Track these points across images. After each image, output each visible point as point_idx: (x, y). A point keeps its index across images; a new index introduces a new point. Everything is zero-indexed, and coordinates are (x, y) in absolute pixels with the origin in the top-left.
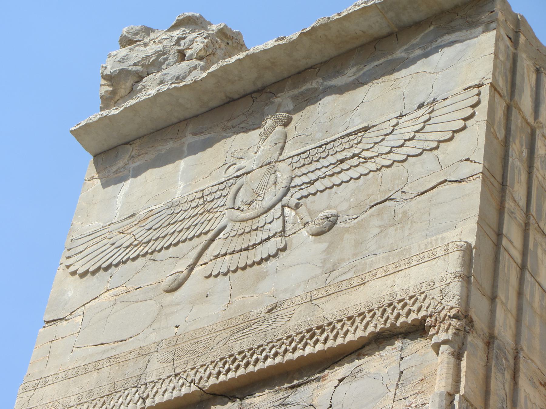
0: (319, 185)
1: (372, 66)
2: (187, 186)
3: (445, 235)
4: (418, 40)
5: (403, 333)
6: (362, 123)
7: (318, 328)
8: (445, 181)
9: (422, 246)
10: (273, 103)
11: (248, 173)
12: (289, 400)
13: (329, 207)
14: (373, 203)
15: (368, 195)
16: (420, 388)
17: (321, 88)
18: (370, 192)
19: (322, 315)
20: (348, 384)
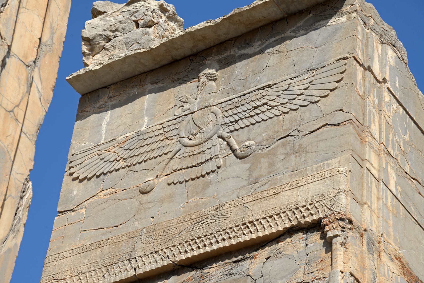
1: (271, 41)
2: (150, 120)
3: (329, 162)
4: (301, 24)
5: (306, 228)
6: (267, 81)
7: (250, 223)
8: (327, 124)
9: (314, 169)
11: (192, 113)
12: (234, 271)
13: (250, 139)
14: (279, 138)
15: (275, 132)
16: (320, 266)
17: (237, 55)
18: (276, 130)
19: (251, 214)
20: (272, 262)
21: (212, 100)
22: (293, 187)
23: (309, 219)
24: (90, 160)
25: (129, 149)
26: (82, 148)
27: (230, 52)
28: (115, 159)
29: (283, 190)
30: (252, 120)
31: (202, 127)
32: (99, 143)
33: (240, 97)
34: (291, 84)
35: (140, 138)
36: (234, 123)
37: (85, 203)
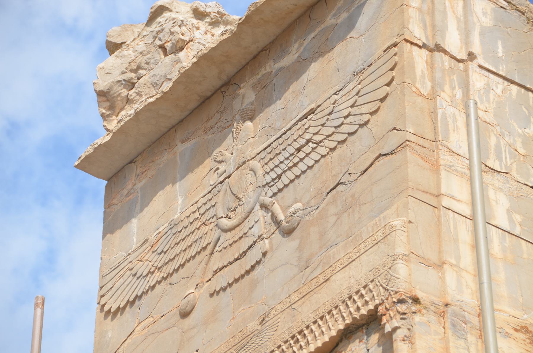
0: (285, 179)
3: (385, 214)
6: (310, 104)
9: (370, 229)
10: (238, 95)
11: (228, 177)
13: (296, 202)
17: (274, 71)
19: (300, 319)
21: (249, 150)
22: (344, 266)
23: (364, 311)
24: (122, 281)
25: (162, 251)
26: (114, 263)
27: (266, 70)
28: (149, 272)
29: (335, 273)
30: (297, 171)
31: (240, 196)
32: (130, 251)
33: (280, 137)
34: (337, 102)
35: (174, 231)
36: (277, 180)
37: (122, 347)
